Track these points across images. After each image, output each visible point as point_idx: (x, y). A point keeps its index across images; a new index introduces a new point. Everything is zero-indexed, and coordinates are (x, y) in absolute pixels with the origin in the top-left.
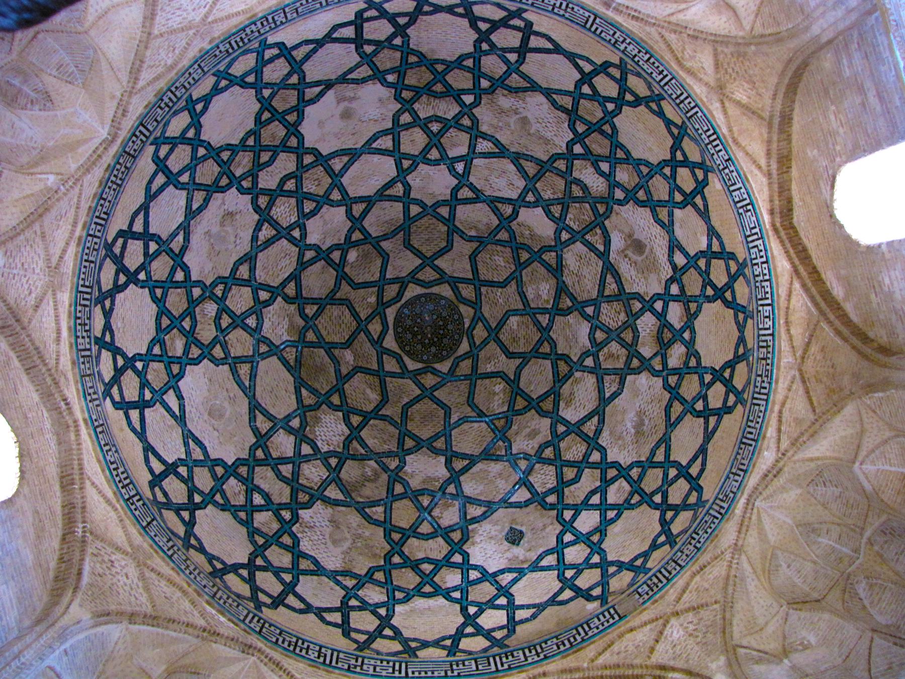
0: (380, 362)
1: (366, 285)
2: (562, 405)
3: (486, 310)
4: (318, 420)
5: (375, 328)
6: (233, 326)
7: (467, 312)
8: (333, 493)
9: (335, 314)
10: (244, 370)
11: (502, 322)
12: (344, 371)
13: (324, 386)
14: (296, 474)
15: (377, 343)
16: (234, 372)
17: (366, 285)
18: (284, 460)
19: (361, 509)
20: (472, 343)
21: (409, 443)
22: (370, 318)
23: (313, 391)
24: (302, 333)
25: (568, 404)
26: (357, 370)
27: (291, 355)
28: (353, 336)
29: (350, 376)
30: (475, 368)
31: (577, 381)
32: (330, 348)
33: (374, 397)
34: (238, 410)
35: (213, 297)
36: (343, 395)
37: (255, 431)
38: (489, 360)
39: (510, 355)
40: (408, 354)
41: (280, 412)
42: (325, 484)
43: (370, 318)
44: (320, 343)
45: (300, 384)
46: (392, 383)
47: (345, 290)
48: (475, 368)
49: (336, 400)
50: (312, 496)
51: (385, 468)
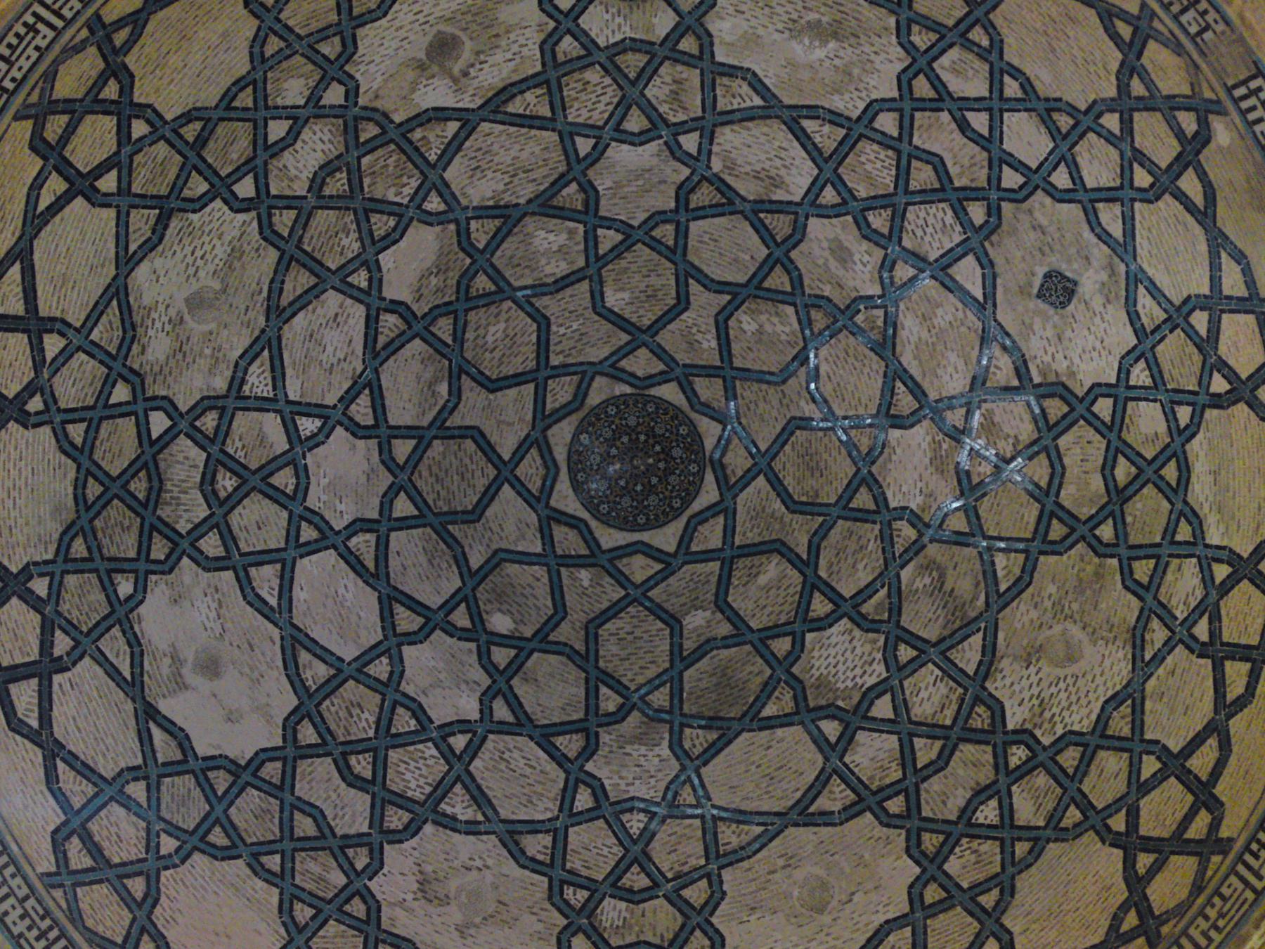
0: (706, 556)
1: (557, 591)
2: (779, 195)
3: (597, 354)
4: (821, 683)
5: (640, 568)
6: (644, 860)
7: (601, 390)
8: (969, 655)
9: (615, 649)
10: (730, 836)
11: (618, 321)
12: (725, 629)
13: (755, 671)
14: (933, 730)
15: (668, 563)
16: (737, 856)
17: (557, 591)
18: (906, 756)
19: (1001, 599)
20: (662, 378)
21: (863, 499)
22: (622, 579)
23: (767, 690)
24: (654, 717)
25: (776, 182)
26: (722, 604)
27: (696, 739)
28: (658, 611)
29: (733, 617)
30: (709, 372)
31: (731, 167)
32: (681, 659)
33: (773, 568)
34: (810, 848)
35: (589, 908)
36: (774, 631)
37: (850, 812)
38: (692, 344)
39: (682, 302)
40: (687, 503)
41: (809, 762)
42: (952, 672)
43: (622, 579)
44: (673, 678)
45: (755, 720)
46: (746, 533)
47: (568, 632)
48: (709, 372)
49: (782, 646)
50: (977, 700)
51: (916, 548)
